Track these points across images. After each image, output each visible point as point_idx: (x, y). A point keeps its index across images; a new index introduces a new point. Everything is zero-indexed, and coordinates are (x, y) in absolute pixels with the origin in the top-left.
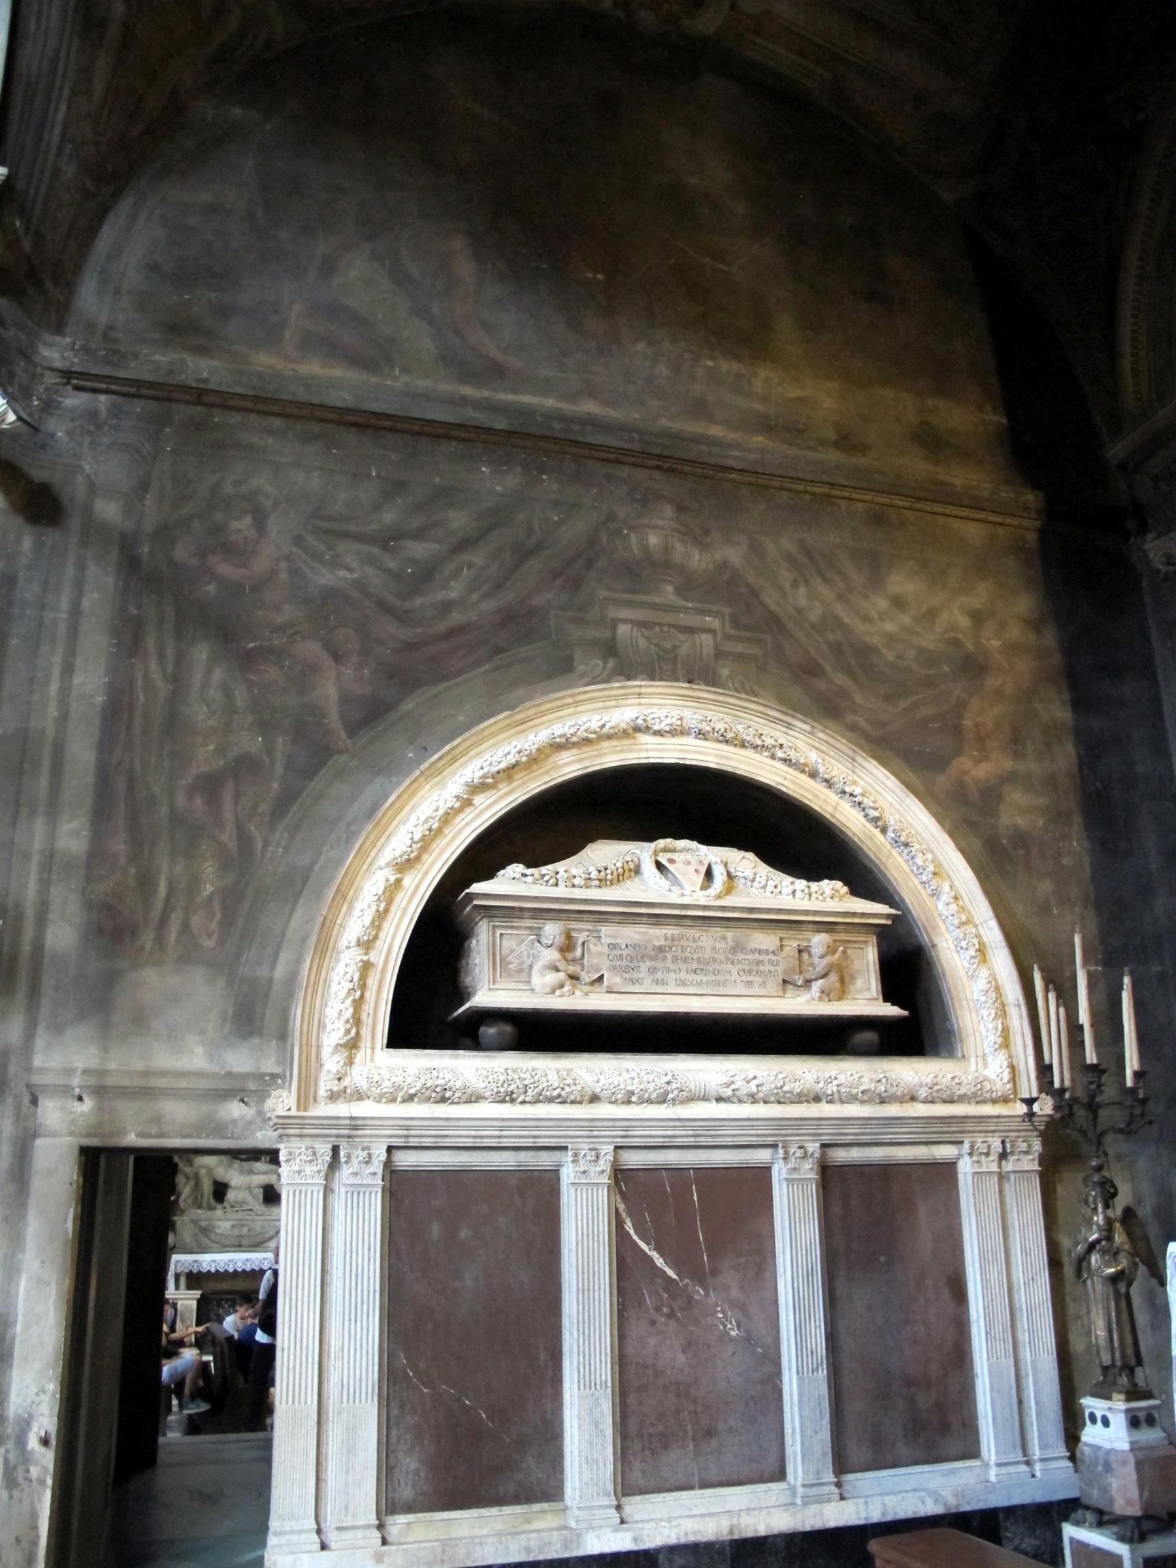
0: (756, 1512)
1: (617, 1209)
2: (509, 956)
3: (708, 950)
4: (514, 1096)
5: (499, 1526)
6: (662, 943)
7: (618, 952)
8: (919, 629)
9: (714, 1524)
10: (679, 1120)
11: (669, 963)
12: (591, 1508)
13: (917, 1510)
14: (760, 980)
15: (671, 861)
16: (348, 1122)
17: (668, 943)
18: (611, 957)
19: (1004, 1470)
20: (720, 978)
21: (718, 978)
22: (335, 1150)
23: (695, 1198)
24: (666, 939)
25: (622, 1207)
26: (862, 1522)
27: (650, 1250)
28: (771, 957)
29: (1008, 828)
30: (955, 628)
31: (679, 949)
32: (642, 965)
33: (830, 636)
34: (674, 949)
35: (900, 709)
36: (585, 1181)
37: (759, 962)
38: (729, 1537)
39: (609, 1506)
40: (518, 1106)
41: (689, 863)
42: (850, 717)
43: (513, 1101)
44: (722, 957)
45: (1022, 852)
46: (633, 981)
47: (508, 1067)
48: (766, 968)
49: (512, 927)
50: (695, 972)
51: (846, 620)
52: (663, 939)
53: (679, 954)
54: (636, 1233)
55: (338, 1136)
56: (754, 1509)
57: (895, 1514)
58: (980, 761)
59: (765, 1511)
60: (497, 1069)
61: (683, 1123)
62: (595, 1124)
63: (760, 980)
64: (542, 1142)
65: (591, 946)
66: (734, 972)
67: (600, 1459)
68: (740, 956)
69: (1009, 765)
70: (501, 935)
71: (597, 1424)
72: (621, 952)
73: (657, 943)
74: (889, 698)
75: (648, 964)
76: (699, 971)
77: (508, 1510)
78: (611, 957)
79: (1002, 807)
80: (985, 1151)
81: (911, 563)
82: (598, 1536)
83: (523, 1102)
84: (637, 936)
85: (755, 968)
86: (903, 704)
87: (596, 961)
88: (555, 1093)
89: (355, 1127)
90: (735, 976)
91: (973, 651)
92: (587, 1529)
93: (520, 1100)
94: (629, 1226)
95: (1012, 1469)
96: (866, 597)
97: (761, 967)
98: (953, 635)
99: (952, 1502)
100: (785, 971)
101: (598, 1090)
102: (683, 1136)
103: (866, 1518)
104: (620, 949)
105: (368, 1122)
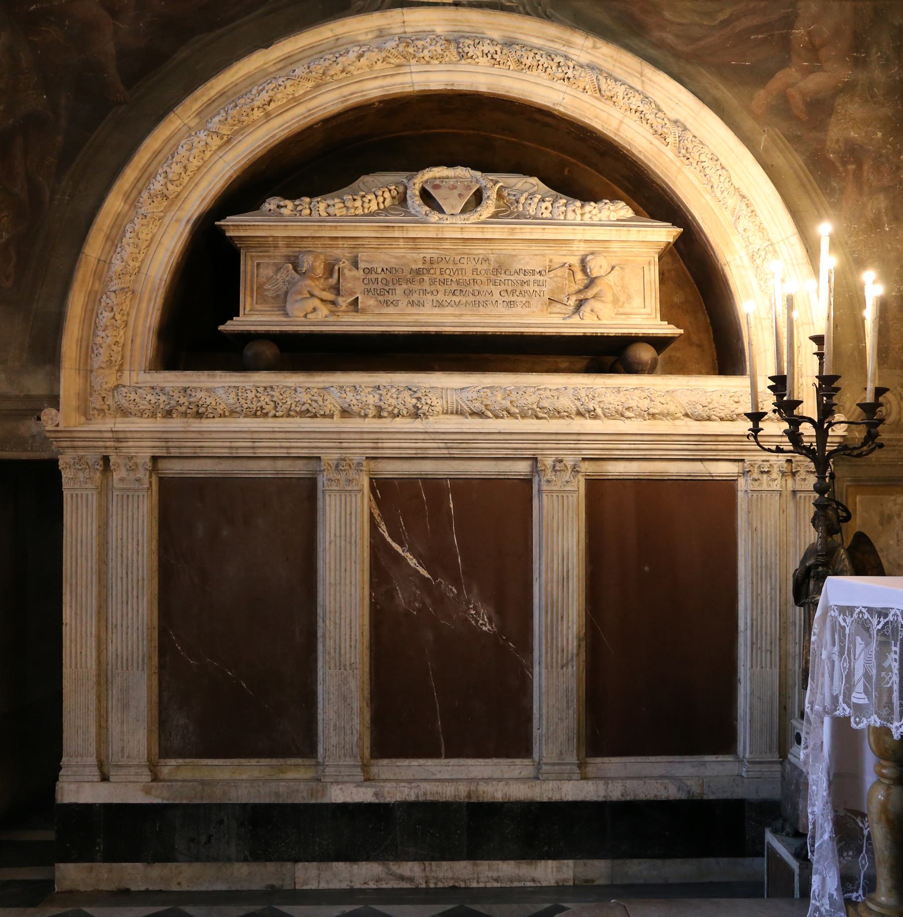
0: (495, 783)
1: (371, 515)
2: (265, 284)
3: (469, 272)
4: (264, 411)
5: (256, 774)
6: (421, 267)
7: (374, 276)
9: (453, 788)
10: (426, 432)
11: (426, 286)
12: (338, 766)
13: (658, 794)
14: (524, 300)
15: (436, 187)
16: (110, 435)
17: (425, 266)
18: (366, 281)
19: (757, 768)
20: (481, 298)
21: (479, 298)
22: (106, 459)
23: (452, 506)
24: (424, 262)
25: (376, 512)
26: (601, 799)
27: (403, 551)
28: (538, 277)
31: (438, 272)
32: (397, 287)
34: (432, 271)
35: (717, 22)
36: (337, 488)
37: (523, 283)
38: (466, 800)
39: (356, 766)
40: (270, 420)
41: (454, 187)
43: (266, 415)
44: (484, 279)
46: (387, 303)
47: (257, 384)
48: (531, 288)
49: (269, 257)
50: (454, 294)
52: (421, 262)
53: (438, 276)
54: (390, 536)
55: (106, 447)
56: (495, 779)
57: (635, 795)
59: (503, 783)
60: (247, 387)
61: (433, 436)
62: (343, 436)
63: (524, 300)
64: (294, 452)
65: (346, 271)
66: (496, 292)
67: (348, 727)
68: (503, 277)
69: (845, 74)
70: (258, 264)
71: (345, 698)
72: (376, 276)
73: (414, 267)
75: (404, 286)
76: (457, 293)
77: (264, 761)
78: (366, 281)
79: (833, 120)
80: (766, 470)
82: (341, 789)
83: (275, 416)
84: (393, 260)
85: (519, 288)
87: (350, 285)
88: (304, 408)
89: (118, 440)
90: (496, 296)
92: (332, 783)
93: (271, 414)
94: (383, 529)
95: (765, 768)
97: (526, 288)
99: (696, 790)
100: (552, 291)
101: (346, 405)
102: (433, 447)
103: (605, 797)
104: (376, 273)
105: (129, 435)
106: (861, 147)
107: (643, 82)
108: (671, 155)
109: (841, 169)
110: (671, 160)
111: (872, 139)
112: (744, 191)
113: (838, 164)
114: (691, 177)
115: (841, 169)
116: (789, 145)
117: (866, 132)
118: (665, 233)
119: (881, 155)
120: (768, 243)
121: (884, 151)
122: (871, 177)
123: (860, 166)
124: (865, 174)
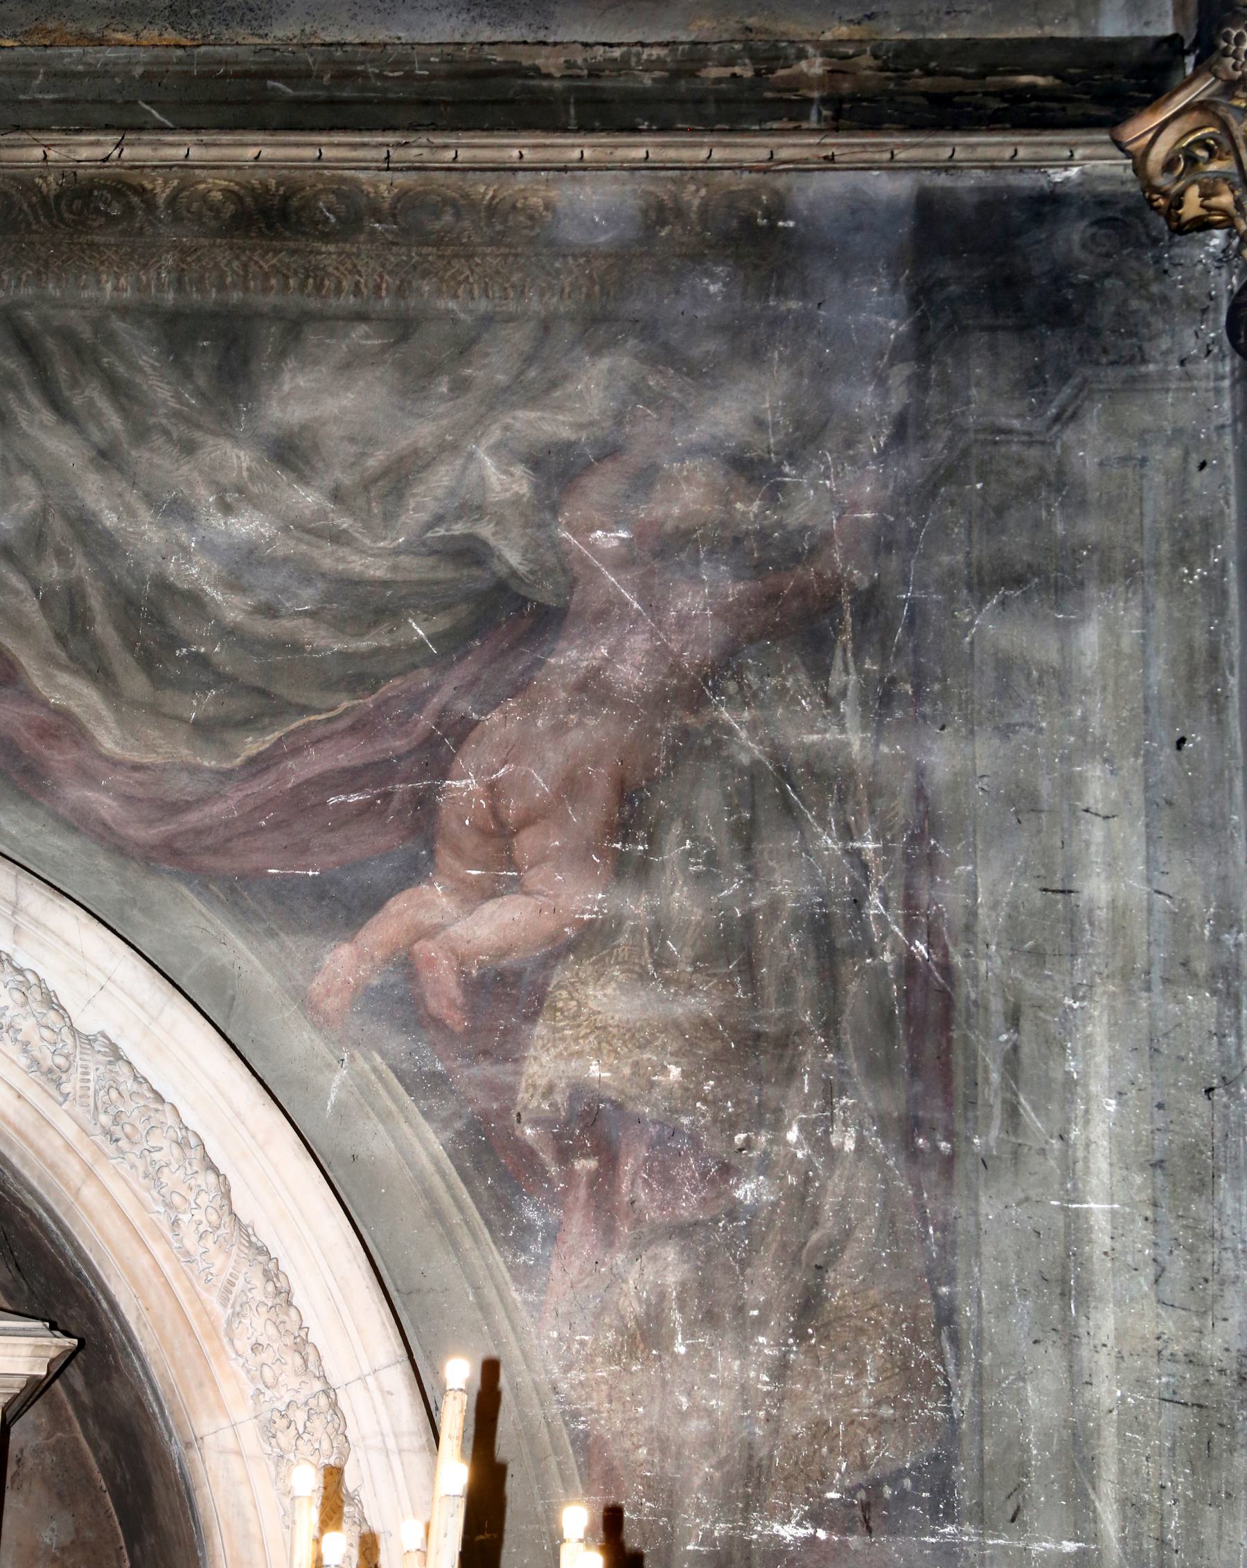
8: (345, 523)
29: (550, 1089)
30: (473, 509)
33: (53, 572)
42: (76, 793)
45: (585, 1165)
51: (110, 519)
58: (494, 895)
74: (205, 730)
79: (540, 1029)
81: (363, 328)
86: (253, 745)
91: (522, 569)
96: (189, 448)
98: (459, 529)
106: (619, 1106)
107: (16, 928)
108: (69, 1130)
109: (553, 1170)
110: (69, 1147)
111: (652, 1085)
112: (265, 1235)
113: (546, 1157)
114: (115, 1188)
115: (553, 1170)
116: (408, 1100)
117: (636, 1064)
118: (26, 1351)
119: (675, 1132)
120: (318, 1386)
121: (685, 1121)
122: (643, 1195)
123: (609, 1159)
124: (625, 1186)
